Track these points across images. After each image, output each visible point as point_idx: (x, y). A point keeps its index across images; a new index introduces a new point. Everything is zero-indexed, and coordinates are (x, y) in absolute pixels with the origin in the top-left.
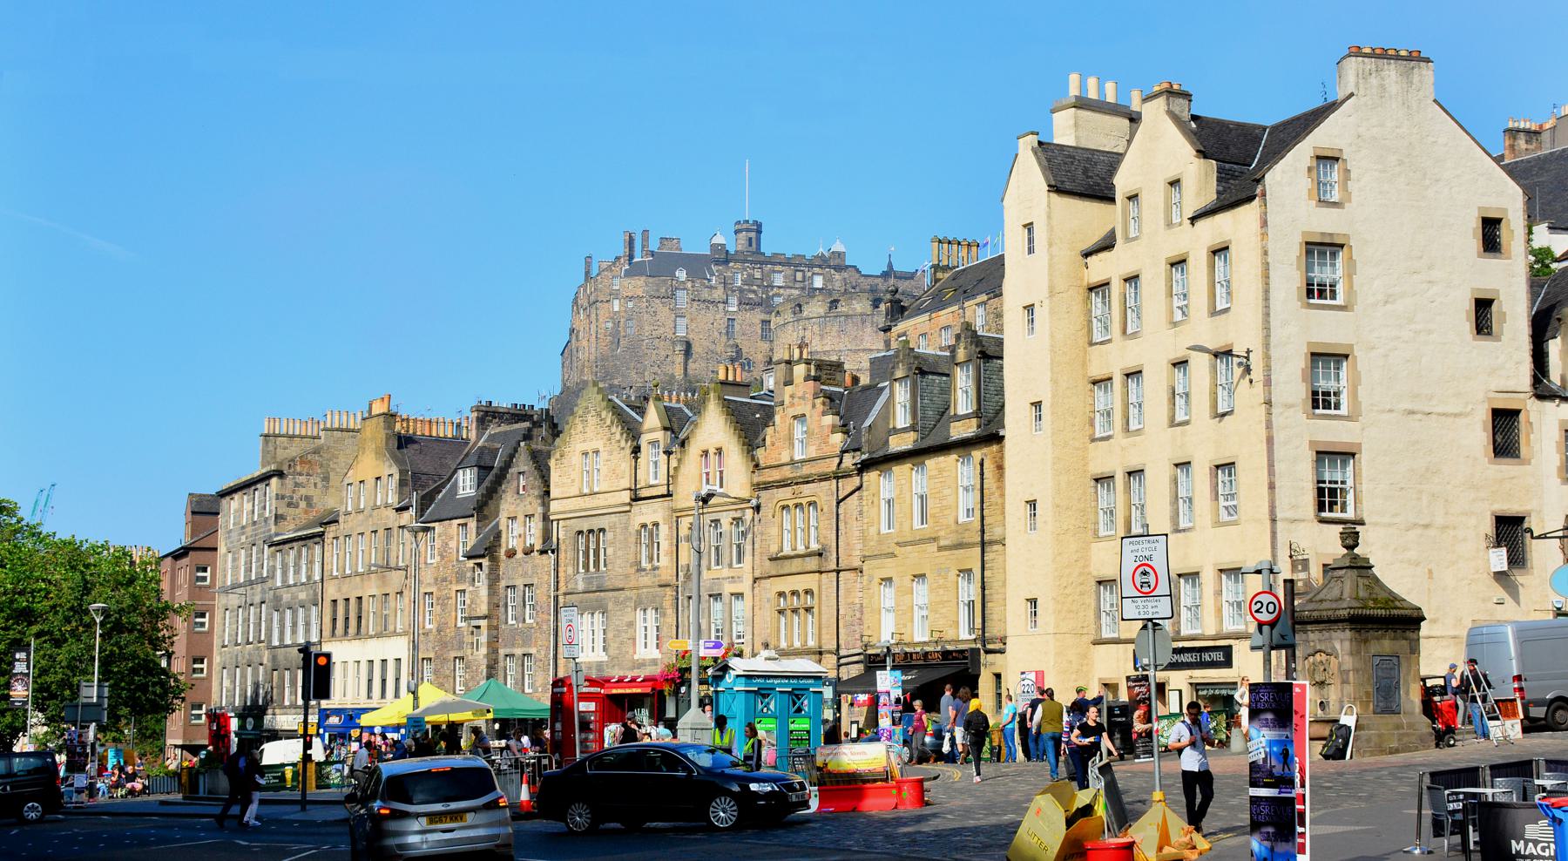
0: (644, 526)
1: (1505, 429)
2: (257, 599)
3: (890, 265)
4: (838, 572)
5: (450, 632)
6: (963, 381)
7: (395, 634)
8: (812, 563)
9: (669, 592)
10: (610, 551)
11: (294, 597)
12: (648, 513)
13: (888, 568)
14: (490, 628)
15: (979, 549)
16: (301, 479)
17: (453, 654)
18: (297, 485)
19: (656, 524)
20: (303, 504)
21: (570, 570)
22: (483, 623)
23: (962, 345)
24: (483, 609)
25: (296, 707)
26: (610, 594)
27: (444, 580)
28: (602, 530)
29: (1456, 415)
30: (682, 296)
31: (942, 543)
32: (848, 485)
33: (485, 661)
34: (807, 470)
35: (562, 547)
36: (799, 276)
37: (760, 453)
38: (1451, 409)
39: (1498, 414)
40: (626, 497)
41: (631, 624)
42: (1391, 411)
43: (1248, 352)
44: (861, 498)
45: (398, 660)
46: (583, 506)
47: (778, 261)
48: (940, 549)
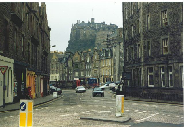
3: (111, 23)
5: (63, 74)
6: (110, 53)
8: (97, 68)
13: (104, 69)
24: (67, 71)
30: (85, 29)
36: (99, 25)
47: (96, 23)
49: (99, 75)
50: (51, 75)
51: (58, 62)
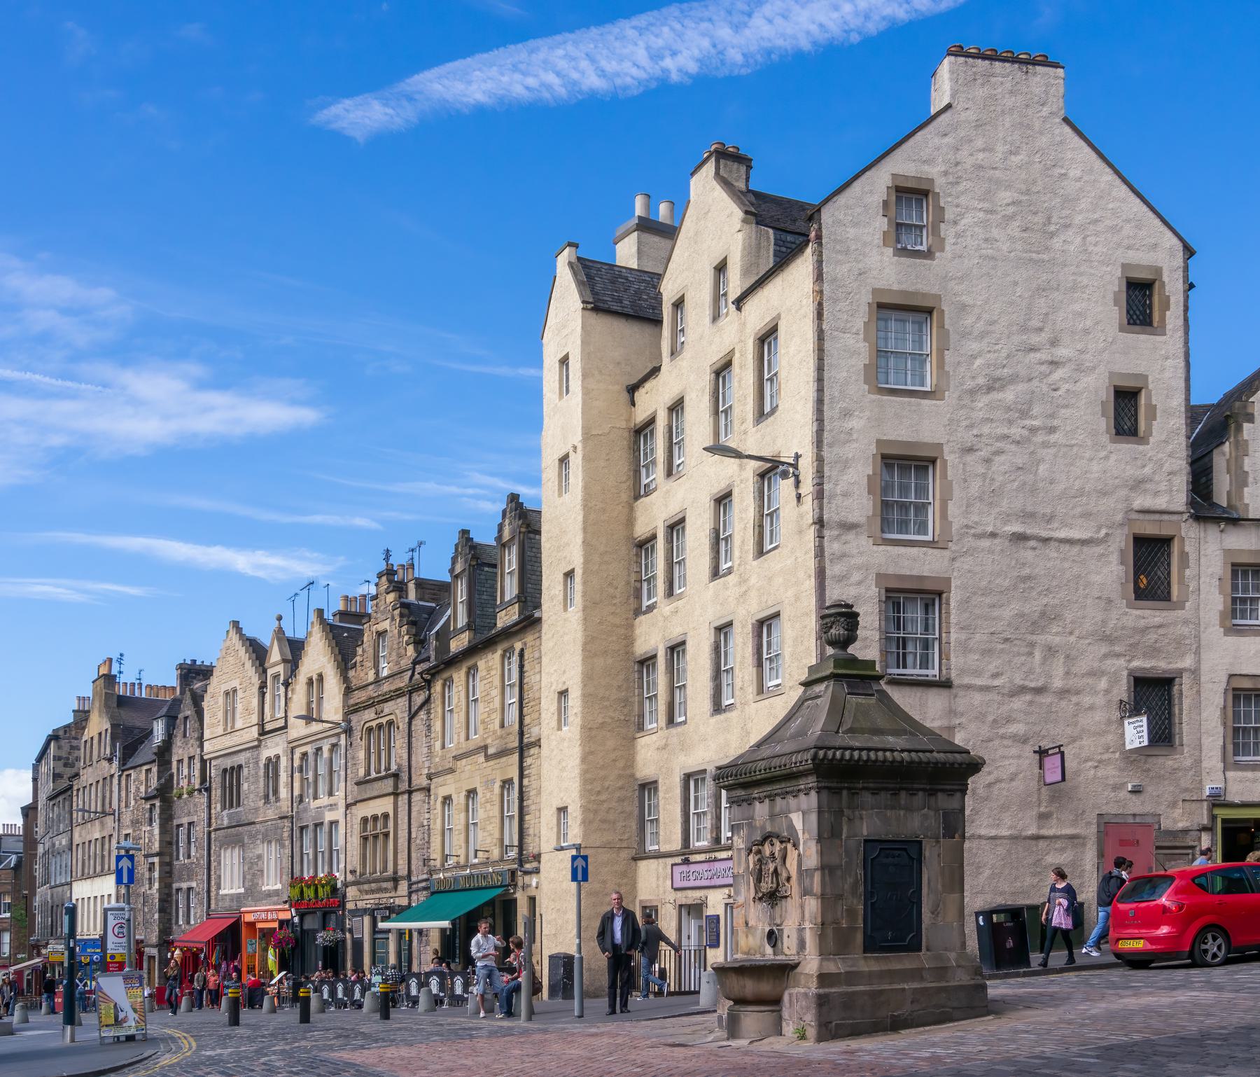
0: (269, 759)
1: (1151, 563)
4: (410, 793)
8: (388, 785)
9: (287, 823)
10: (245, 786)
12: (274, 747)
14: (161, 864)
15: (516, 756)
19: (278, 757)
21: (219, 806)
22: (156, 860)
23: (507, 521)
24: (156, 847)
26: (246, 828)
27: (137, 822)
28: (240, 767)
29: (1084, 542)
31: (491, 751)
32: (419, 699)
33: (157, 895)
34: (386, 687)
35: (214, 786)
37: (351, 673)
38: (1075, 534)
39: (1141, 542)
41: (260, 857)
42: (993, 535)
43: (797, 457)
44: (429, 713)
46: (228, 744)
48: (488, 758)
49: (403, 871)
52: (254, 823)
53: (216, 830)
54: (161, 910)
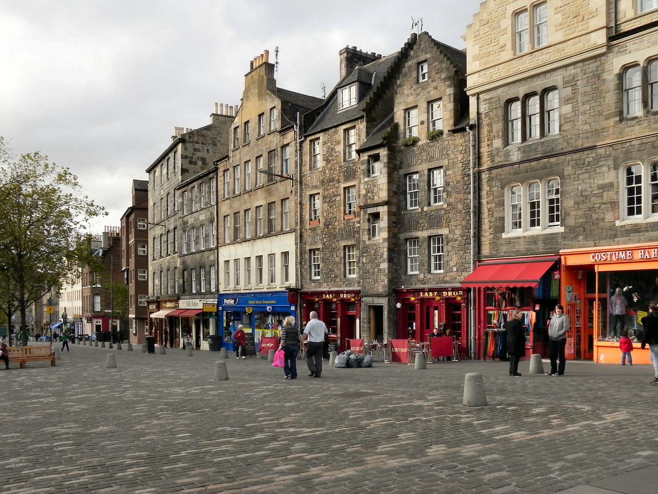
2: (172, 227)
7: (282, 232)
11: (197, 219)
14: (390, 214)
16: (197, 146)
17: (343, 243)
18: (195, 150)
20: (200, 163)
21: (498, 143)
24: (383, 195)
25: (212, 293)
33: (386, 244)
35: (485, 121)
40: (600, 38)
45: (286, 254)
46: (522, 67)
50: (225, 253)
51: (283, 131)
52: (593, 148)
53: (490, 169)
54: (390, 260)
